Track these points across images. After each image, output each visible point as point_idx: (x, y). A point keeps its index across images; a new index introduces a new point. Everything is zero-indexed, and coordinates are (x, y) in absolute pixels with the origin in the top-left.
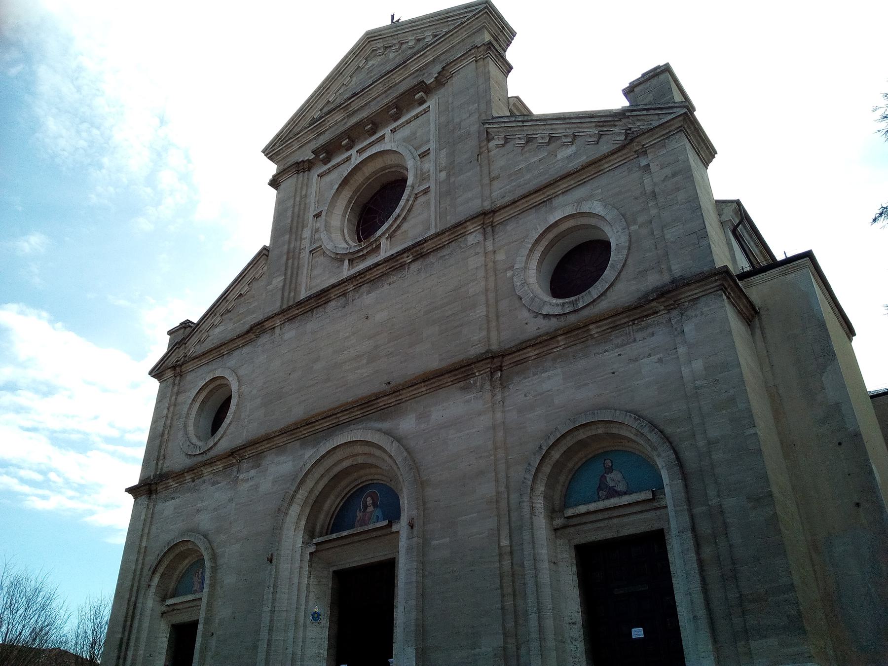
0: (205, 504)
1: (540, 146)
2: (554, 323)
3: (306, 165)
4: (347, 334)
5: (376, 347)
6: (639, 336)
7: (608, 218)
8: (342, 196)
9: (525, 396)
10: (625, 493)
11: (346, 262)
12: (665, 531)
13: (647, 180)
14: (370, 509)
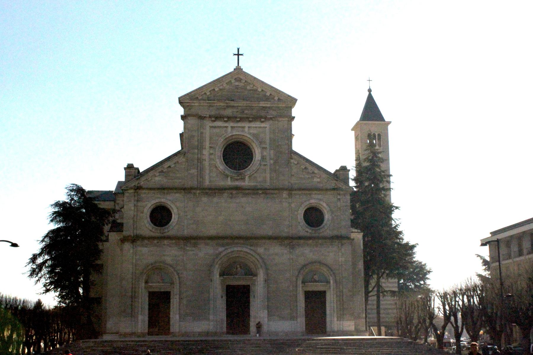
1: (308, 173)
3: (203, 117)
11: (229, 178)
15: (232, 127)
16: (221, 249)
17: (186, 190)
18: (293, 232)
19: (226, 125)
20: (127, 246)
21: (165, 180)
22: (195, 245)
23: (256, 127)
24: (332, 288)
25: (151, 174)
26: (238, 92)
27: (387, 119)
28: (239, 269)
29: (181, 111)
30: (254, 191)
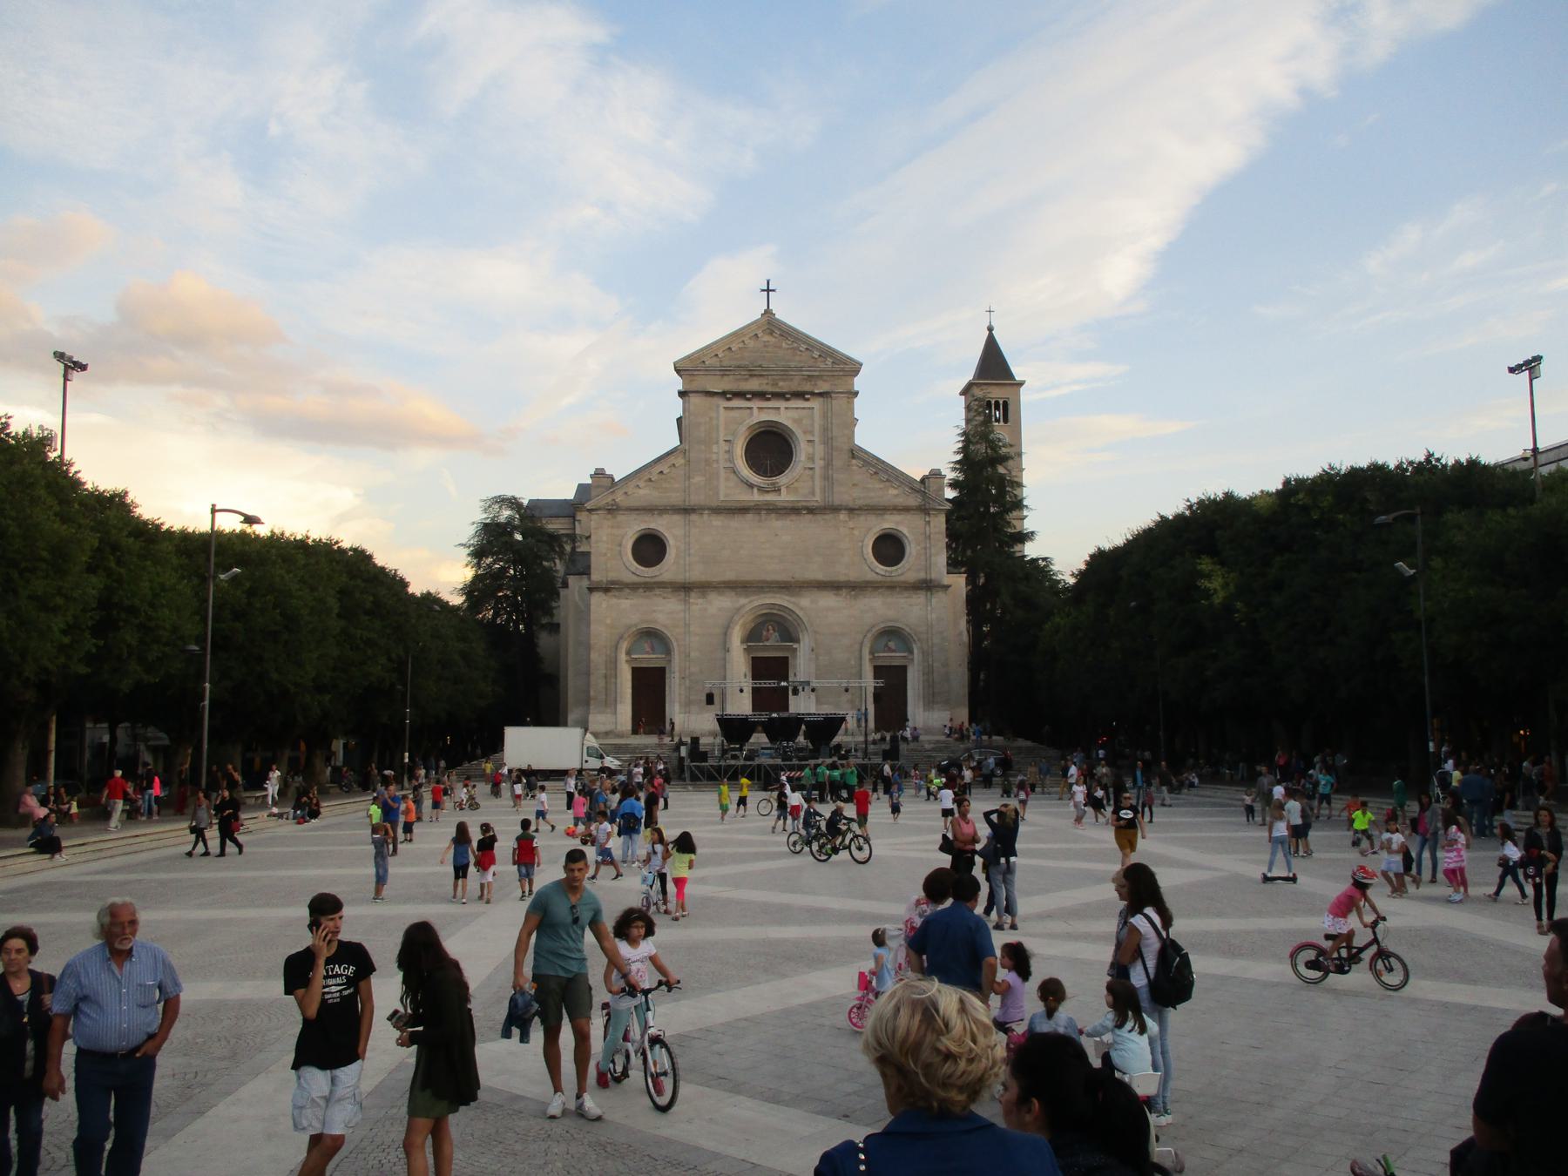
2: (879, 578)
6: (914, 596)
7: (910, 539)
11: (755, 490)
13: (928, 529)
15: (760, 408)
16: (743, 601)
17: (687, 511)
18: (853, 575)
19: (748, 404)
20: (597, 598)
22: (704, 596)
23: (797, 408)
24: (916, 661)
25: (632, 484)
26: (767, 352)
27: (1018, 378)
28: (771, 631)
29: (678, 383)
30: (794, 510)
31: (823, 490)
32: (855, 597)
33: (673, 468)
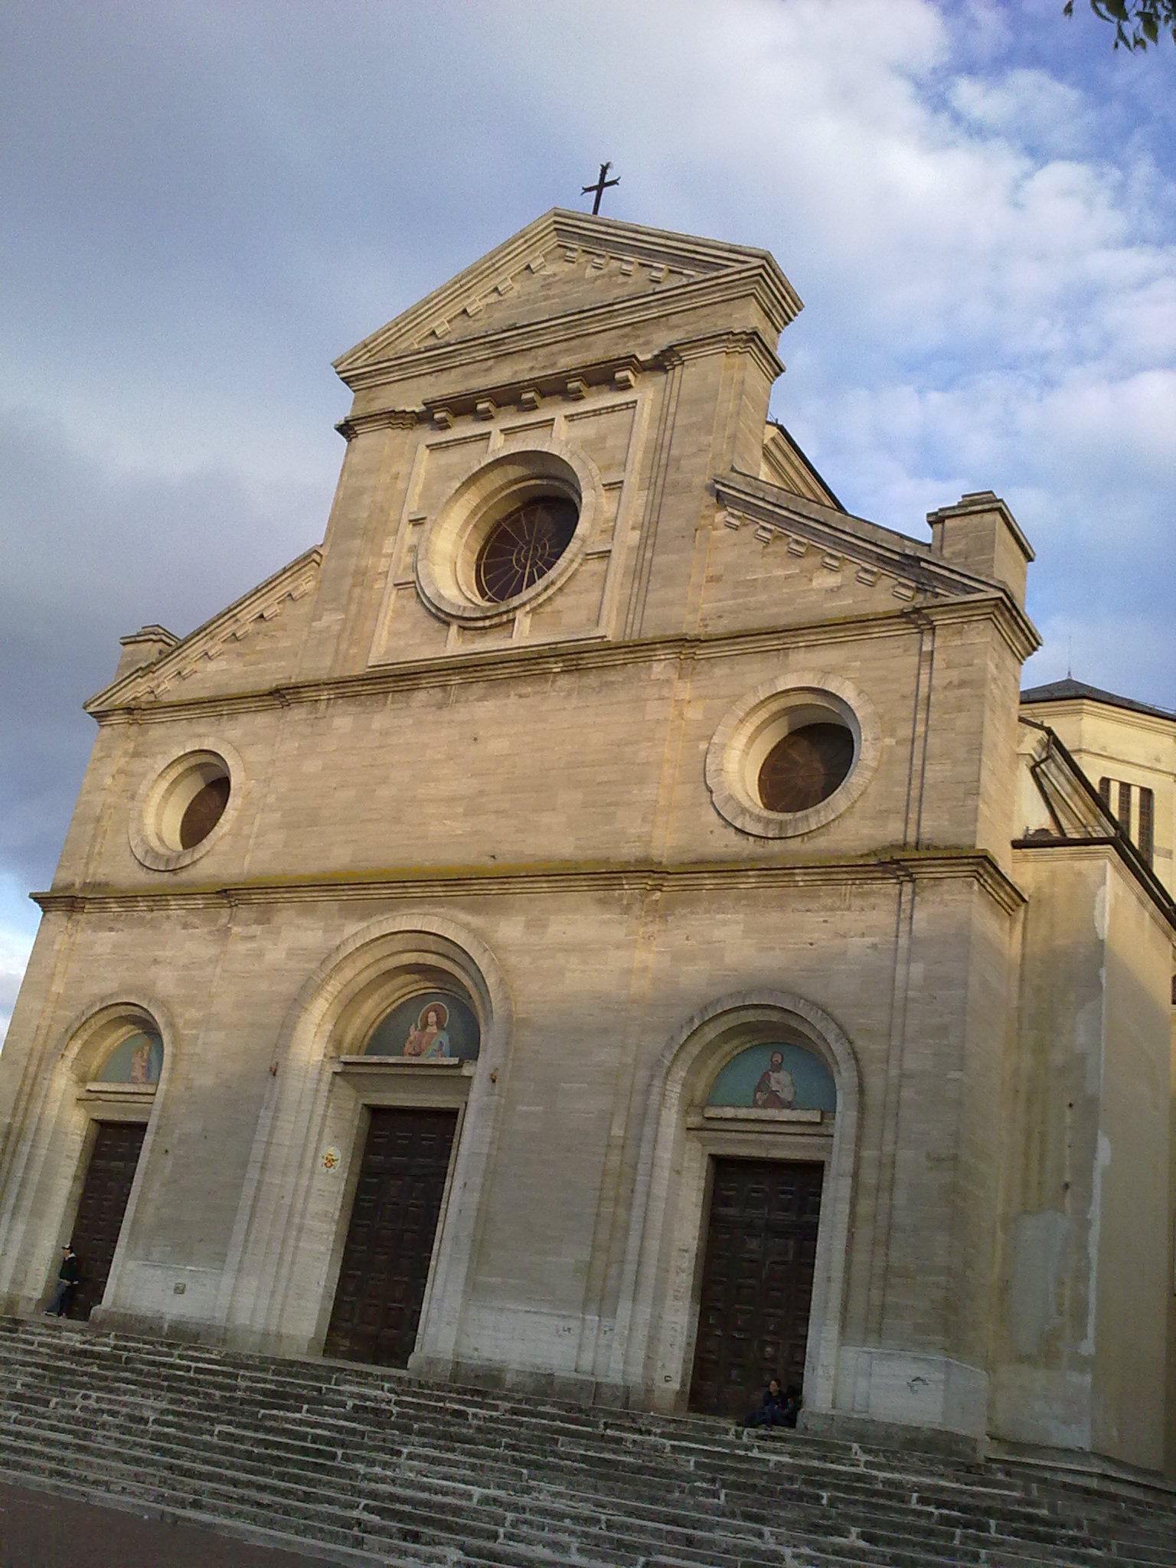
0: (169, 954)
2: (748, 847)
4: (439, 756)
5: (481, 793)
6: (857, 903)
8: (463, 501)
9: (687, 939)
10: (789, 1106)
11: (454, 629)
12: (826, 1164)
14: (433, 1029)
21: (238, 667)
28: (433, 1029)
31: (626, 608)
32: (661, 913)
33: (289, 603)
